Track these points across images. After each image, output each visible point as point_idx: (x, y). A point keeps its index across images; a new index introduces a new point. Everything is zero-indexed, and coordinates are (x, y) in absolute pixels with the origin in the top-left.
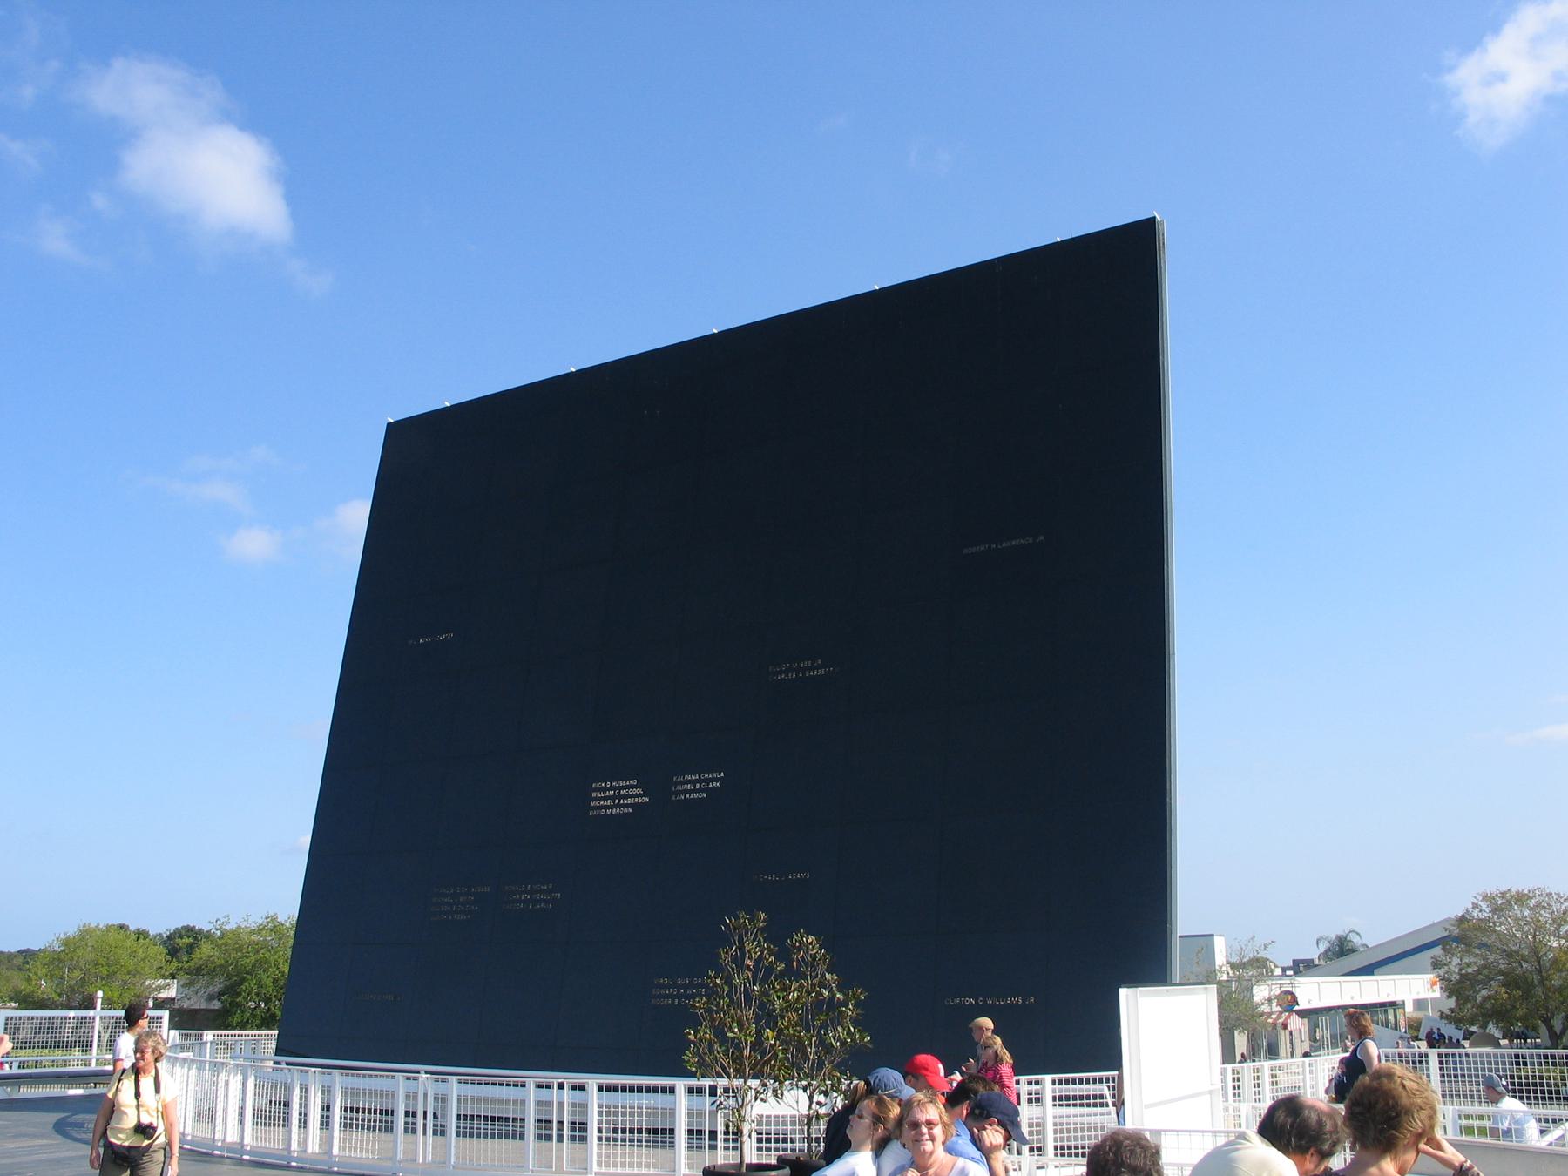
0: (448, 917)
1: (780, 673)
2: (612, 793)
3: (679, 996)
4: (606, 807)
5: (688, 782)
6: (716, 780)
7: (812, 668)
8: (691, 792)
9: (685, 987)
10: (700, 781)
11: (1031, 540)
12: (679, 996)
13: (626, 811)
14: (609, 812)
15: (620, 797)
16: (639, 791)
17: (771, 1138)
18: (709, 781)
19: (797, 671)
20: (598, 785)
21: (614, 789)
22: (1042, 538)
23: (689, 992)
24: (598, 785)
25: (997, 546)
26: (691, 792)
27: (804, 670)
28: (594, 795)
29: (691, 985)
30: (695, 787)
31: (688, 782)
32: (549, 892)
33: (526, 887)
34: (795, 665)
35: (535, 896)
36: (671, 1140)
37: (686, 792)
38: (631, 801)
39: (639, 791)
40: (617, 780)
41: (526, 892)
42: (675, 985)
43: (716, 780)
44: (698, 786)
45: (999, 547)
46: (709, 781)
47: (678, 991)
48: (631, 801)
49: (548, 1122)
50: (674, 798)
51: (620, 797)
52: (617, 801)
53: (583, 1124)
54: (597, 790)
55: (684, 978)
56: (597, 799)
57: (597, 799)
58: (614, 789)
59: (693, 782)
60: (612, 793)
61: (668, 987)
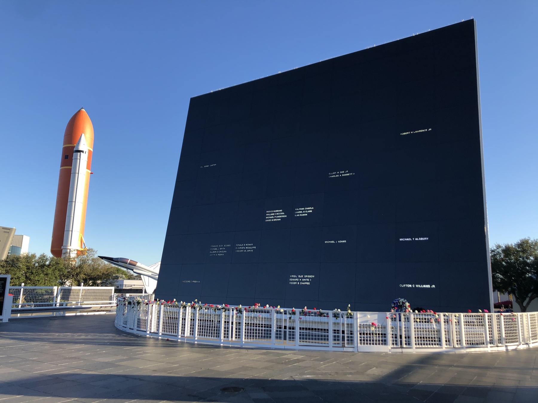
0: (216, 255)
1: (333, 175)
2: (273, 214)
3: (299, 282)
4: (271, 219)
5: (300, 210)
6: (310, 210)
7: (344, 174)
8: (301, 214)
9: (302, 278)
10: (305, 210)
11: (426, 130)
12: (299, 282)
13: (278, 220)
14: (272, 220)
15: (276, 215)
16: (284, 213)
17: (321, 330)
18: (308, 210)
19: (339, 174)
20: (268, 212)
21: (274, 213)
22: (430, 129)
23: (303, 280)
24: (268, 212)
25: (413, 132)
26: (301, 214)
27: (342, 174)
28: (267, 215)
29: (304, 278)
30: (303, 212)
31: (300, 210)
32: (251, 246)
33: (243, 245)
34: (338, 173)
35: (246, 248)
37: (299, 214)
38: (280, 217)
39: (282, 213)
41: (243, 246)
42: (298, 278)
43: (310, 210)
44: (304, 212)
45: (414, 132)
46: (308, 210)
47: (299, 280)
48: (280, 217)
49: (338, 331)
50: (295, 215)
51: (276, 215)
52: (275, 217)
54: (268, 213)
55: (301, 275)
58: (274, 213)
59: (303, 211)
60: (273, 214)
61: (295, 278)
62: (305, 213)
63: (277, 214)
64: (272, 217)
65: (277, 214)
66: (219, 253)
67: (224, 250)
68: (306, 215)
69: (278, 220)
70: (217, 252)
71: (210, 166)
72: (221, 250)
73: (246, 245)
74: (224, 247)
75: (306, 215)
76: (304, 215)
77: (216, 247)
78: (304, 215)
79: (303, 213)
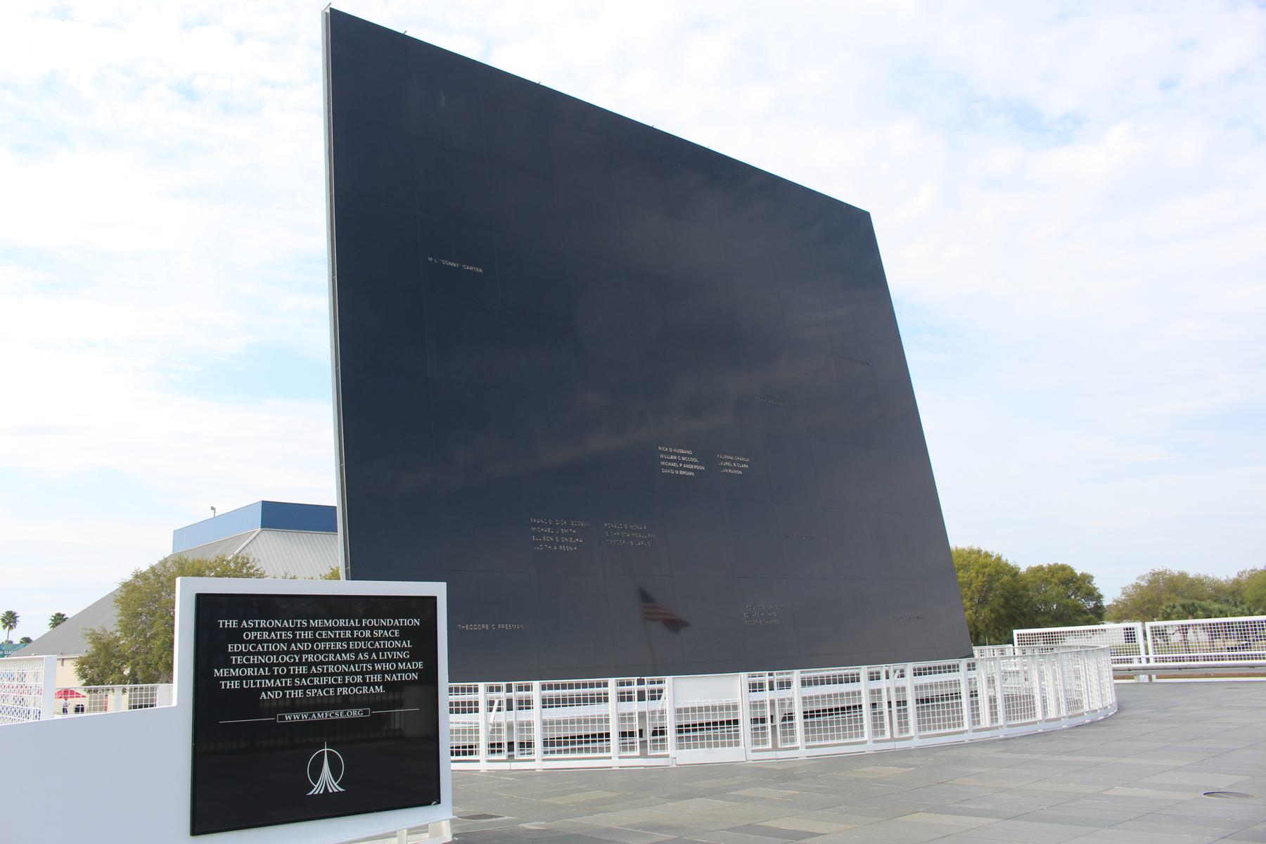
0: (553, 548)
2: (675, 458)
13: (690, 474)
14: (677, 472)
15: (684, 462)
21: (677, 454)
33: (624, 527)
36: (861, 713)
37: (727, 467)
38: (692, 467)
40: (678, 448)
48: (692, 467)
53: (664, 727)
56: (664, 460)
57: (664, 460)
58: (677, 454)
59: (732, 461)
60: (675, 458)
62: (736, 468)
63: (684, 459)
64: (674, 465)
65: (684, 459)
66: (563, 544)
67: (574, 536)
68: (740, 472)
69: (690, 474)
70: (555, 539)
71: (461, 267)
72: (565, 535)
73: (632, 526)
74: (574, 528)
75: (740, 472)
76: (736, 472)
77: (548, 526)
78: (736, 472)
79: (733, 468)
